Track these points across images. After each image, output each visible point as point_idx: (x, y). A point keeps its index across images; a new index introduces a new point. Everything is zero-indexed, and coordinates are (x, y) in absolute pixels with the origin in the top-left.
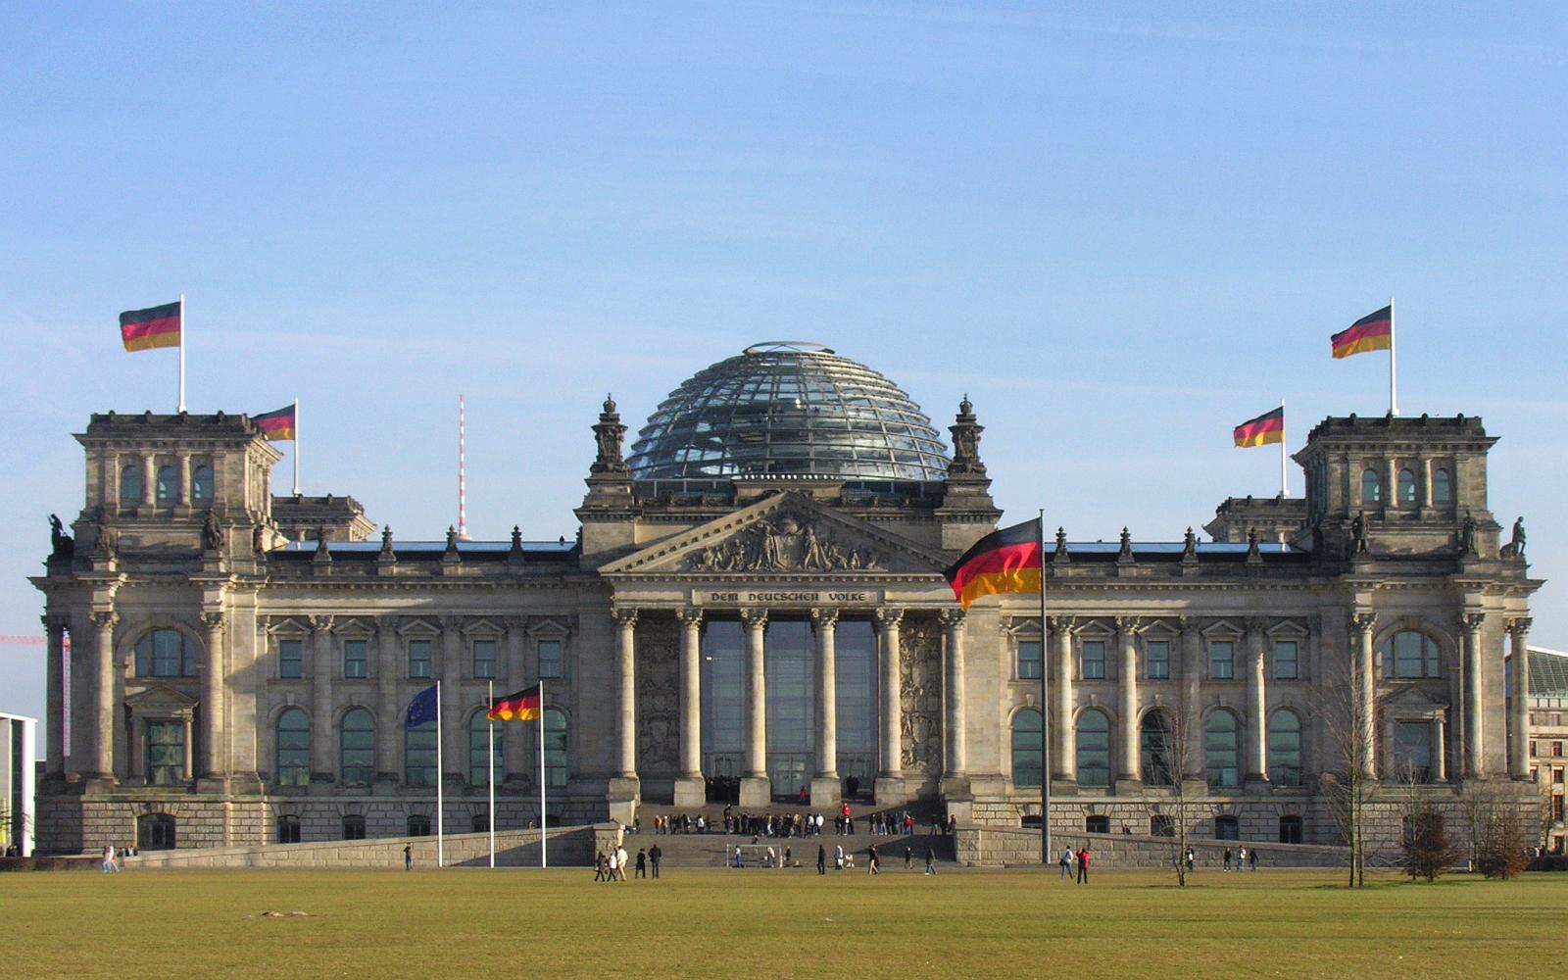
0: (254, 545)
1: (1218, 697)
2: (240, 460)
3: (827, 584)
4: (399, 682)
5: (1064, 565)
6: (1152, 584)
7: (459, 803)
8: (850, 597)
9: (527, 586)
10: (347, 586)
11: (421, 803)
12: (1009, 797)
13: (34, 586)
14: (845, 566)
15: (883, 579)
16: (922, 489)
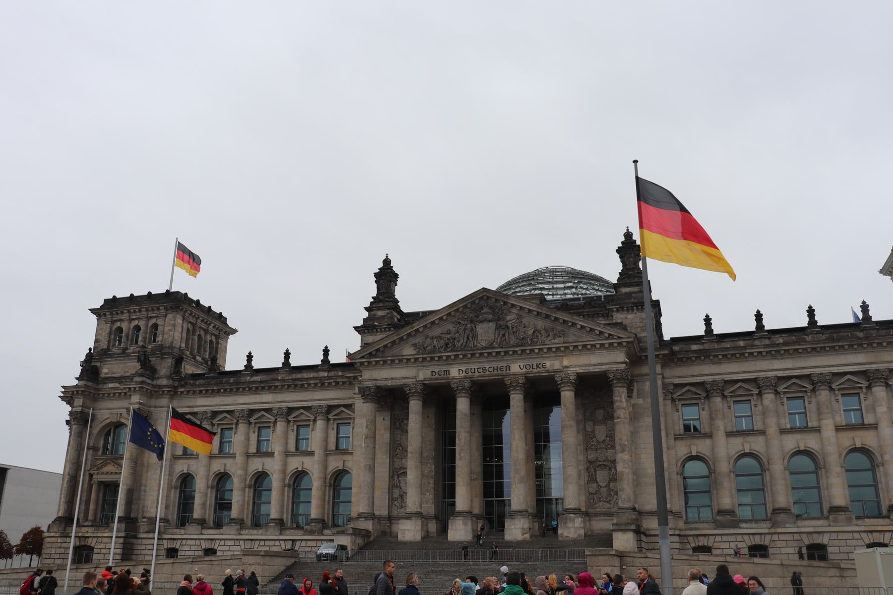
0: (176, 368)
1: (854, 439)
2: (173, 317)
3: (516, 357)
4: (248, 456)
5: (710, 341)
6: (783, 348)
7: (275, 540)
8: (535, 366)
9: (326, 384)
10: (219, 391)
11: (252, 540)
12: (680, 530)
13: (65, 403)
14: (529, 342)
15: (558, 349)
16: (603, 300)
